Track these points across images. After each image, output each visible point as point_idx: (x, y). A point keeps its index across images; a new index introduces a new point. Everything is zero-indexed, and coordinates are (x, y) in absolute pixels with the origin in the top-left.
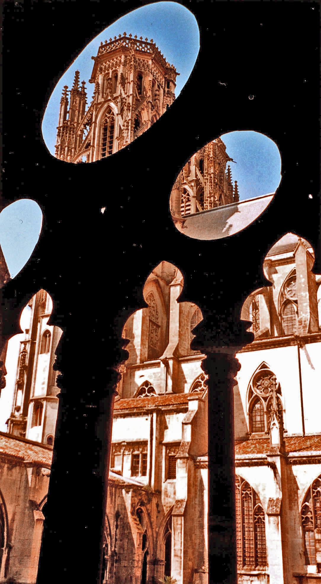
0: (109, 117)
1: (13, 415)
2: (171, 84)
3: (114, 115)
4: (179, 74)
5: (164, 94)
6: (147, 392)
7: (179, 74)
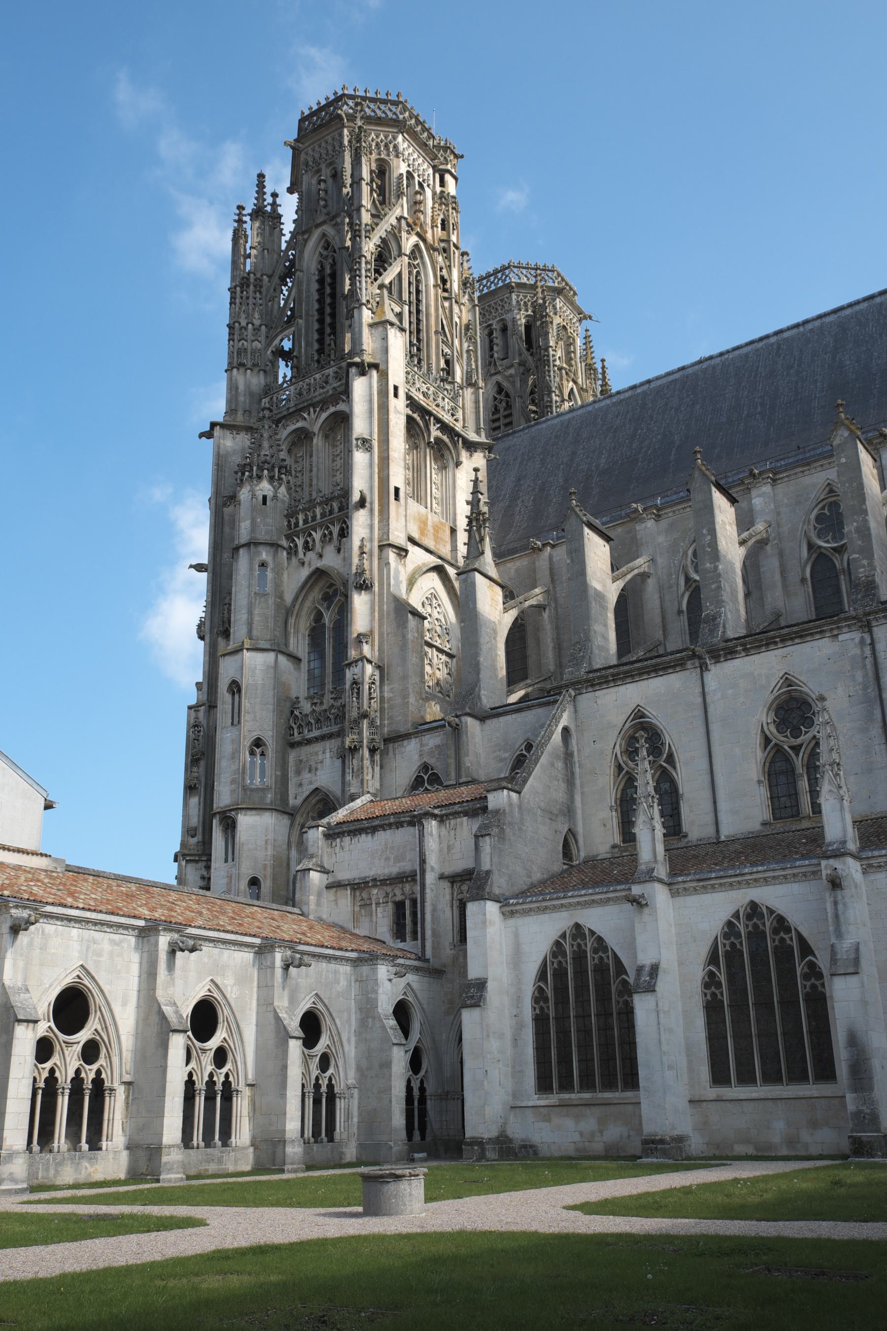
0: (327, 256)
1: (183, 844)
2: (448, 178)
3: (335, 251)
4: (462, 157)
5: (433, 199)
6: (426, 784)
7: (462, 157)
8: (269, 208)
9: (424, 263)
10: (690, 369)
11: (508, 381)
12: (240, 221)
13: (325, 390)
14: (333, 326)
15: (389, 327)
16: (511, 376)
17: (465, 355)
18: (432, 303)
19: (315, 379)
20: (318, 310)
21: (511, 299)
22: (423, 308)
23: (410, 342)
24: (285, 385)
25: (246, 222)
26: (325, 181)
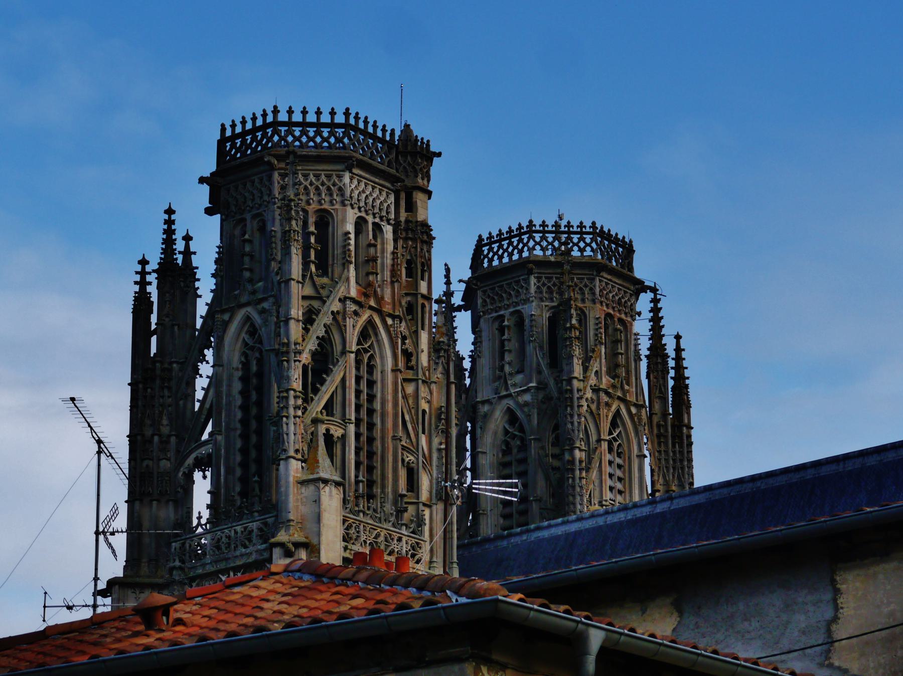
4: (439, 155)
7: (439, 155)
8: (180, 259)
9: (378, 341)
10: (717, 492)
11: (523, 412)
12: (143, 284)
13: (248, 551)
14: (259, 461)
15: (322, 485)
16: (526, 404)
17: (435, 456)
18: (390, 397)
19: (236, 532)
20: (241, 421)
21: (529, 284)
22: (377, 405)
23: (357, 476)
24: (200, 530)
25: (150, 283)
26: (250, 241)
